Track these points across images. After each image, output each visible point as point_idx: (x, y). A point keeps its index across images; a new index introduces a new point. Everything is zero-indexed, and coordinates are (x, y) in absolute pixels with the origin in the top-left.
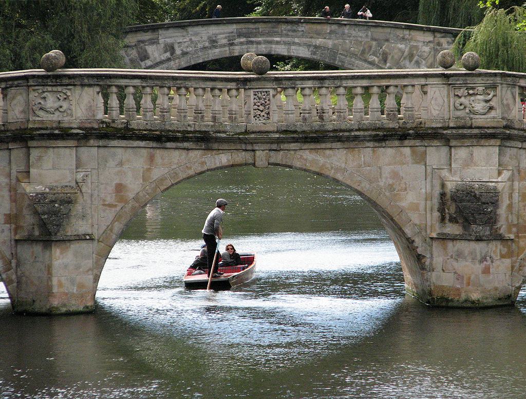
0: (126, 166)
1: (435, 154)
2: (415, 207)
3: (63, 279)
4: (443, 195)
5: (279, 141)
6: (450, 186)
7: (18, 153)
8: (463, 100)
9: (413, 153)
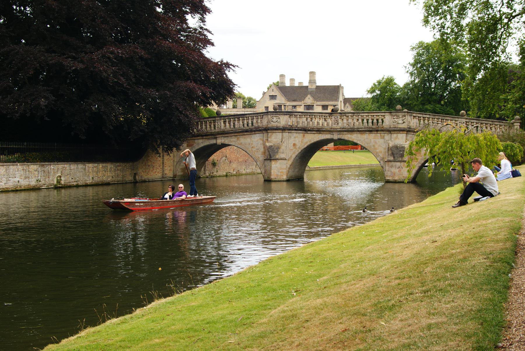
0: (296, 139)
1: (387, 136)
2: (381, 152)
3: (275, 171)
4: (388, 148)
5: (340, 131)
6: (390, 145)
7: (265, 134)
8: (395, 119)
9: (381, 135)
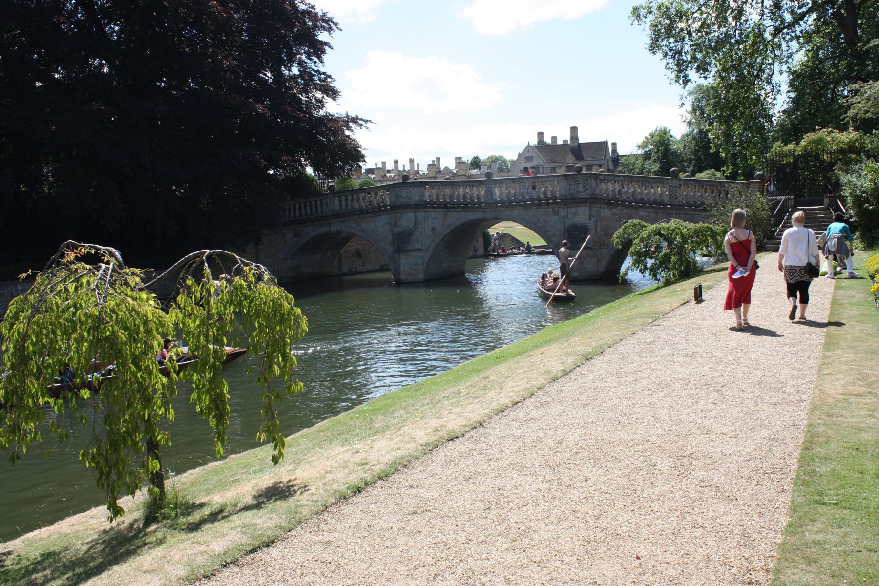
4: (564, 229)
6: (567, 225)
8: (573, 186)
